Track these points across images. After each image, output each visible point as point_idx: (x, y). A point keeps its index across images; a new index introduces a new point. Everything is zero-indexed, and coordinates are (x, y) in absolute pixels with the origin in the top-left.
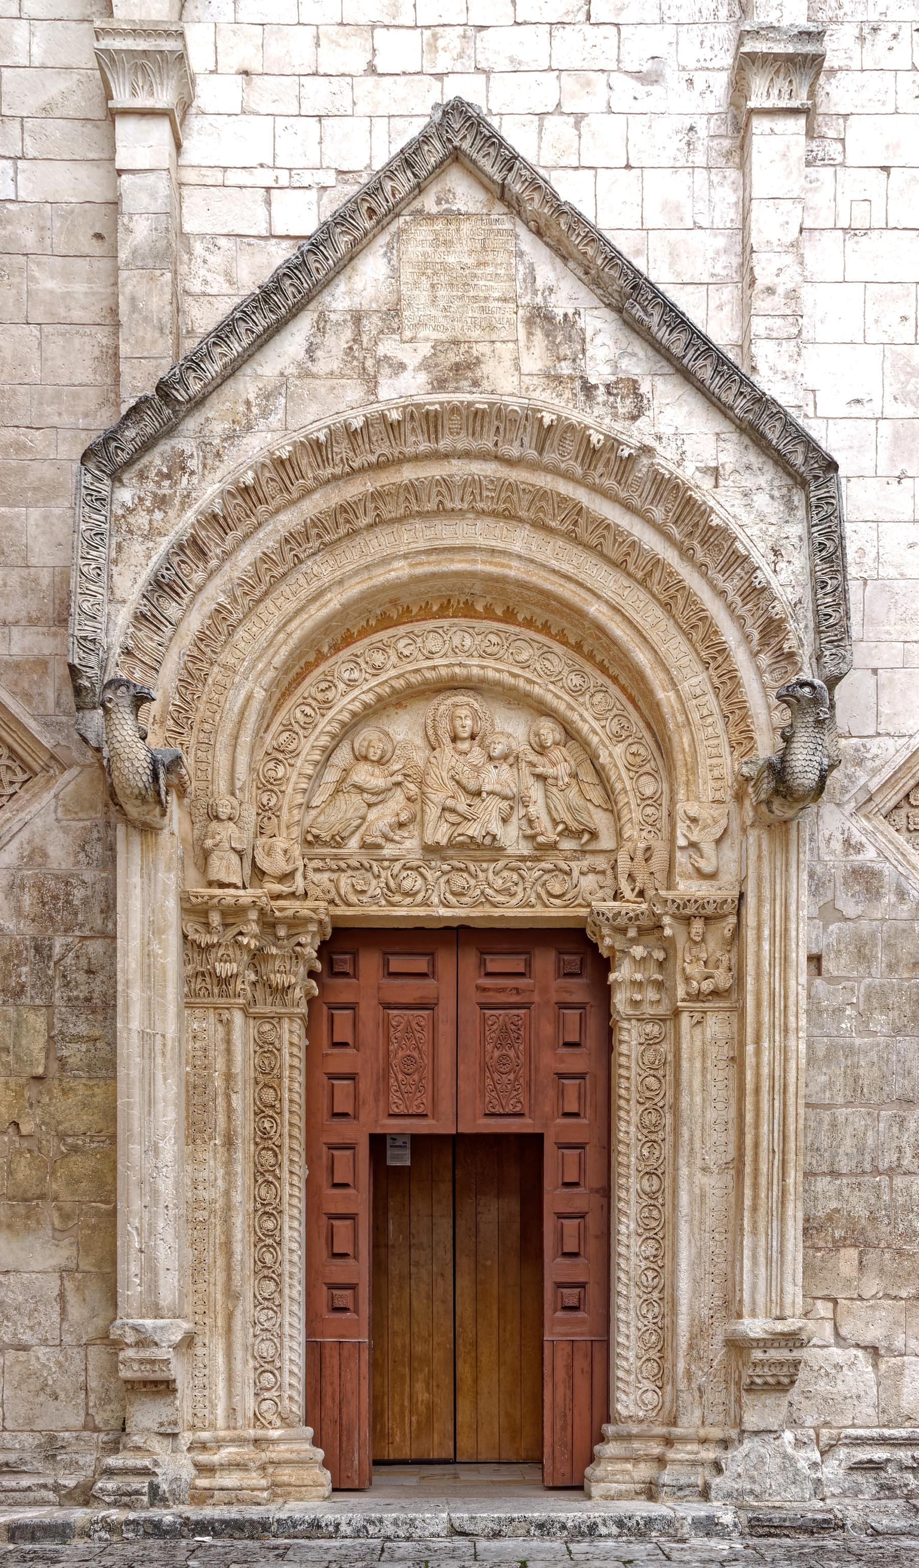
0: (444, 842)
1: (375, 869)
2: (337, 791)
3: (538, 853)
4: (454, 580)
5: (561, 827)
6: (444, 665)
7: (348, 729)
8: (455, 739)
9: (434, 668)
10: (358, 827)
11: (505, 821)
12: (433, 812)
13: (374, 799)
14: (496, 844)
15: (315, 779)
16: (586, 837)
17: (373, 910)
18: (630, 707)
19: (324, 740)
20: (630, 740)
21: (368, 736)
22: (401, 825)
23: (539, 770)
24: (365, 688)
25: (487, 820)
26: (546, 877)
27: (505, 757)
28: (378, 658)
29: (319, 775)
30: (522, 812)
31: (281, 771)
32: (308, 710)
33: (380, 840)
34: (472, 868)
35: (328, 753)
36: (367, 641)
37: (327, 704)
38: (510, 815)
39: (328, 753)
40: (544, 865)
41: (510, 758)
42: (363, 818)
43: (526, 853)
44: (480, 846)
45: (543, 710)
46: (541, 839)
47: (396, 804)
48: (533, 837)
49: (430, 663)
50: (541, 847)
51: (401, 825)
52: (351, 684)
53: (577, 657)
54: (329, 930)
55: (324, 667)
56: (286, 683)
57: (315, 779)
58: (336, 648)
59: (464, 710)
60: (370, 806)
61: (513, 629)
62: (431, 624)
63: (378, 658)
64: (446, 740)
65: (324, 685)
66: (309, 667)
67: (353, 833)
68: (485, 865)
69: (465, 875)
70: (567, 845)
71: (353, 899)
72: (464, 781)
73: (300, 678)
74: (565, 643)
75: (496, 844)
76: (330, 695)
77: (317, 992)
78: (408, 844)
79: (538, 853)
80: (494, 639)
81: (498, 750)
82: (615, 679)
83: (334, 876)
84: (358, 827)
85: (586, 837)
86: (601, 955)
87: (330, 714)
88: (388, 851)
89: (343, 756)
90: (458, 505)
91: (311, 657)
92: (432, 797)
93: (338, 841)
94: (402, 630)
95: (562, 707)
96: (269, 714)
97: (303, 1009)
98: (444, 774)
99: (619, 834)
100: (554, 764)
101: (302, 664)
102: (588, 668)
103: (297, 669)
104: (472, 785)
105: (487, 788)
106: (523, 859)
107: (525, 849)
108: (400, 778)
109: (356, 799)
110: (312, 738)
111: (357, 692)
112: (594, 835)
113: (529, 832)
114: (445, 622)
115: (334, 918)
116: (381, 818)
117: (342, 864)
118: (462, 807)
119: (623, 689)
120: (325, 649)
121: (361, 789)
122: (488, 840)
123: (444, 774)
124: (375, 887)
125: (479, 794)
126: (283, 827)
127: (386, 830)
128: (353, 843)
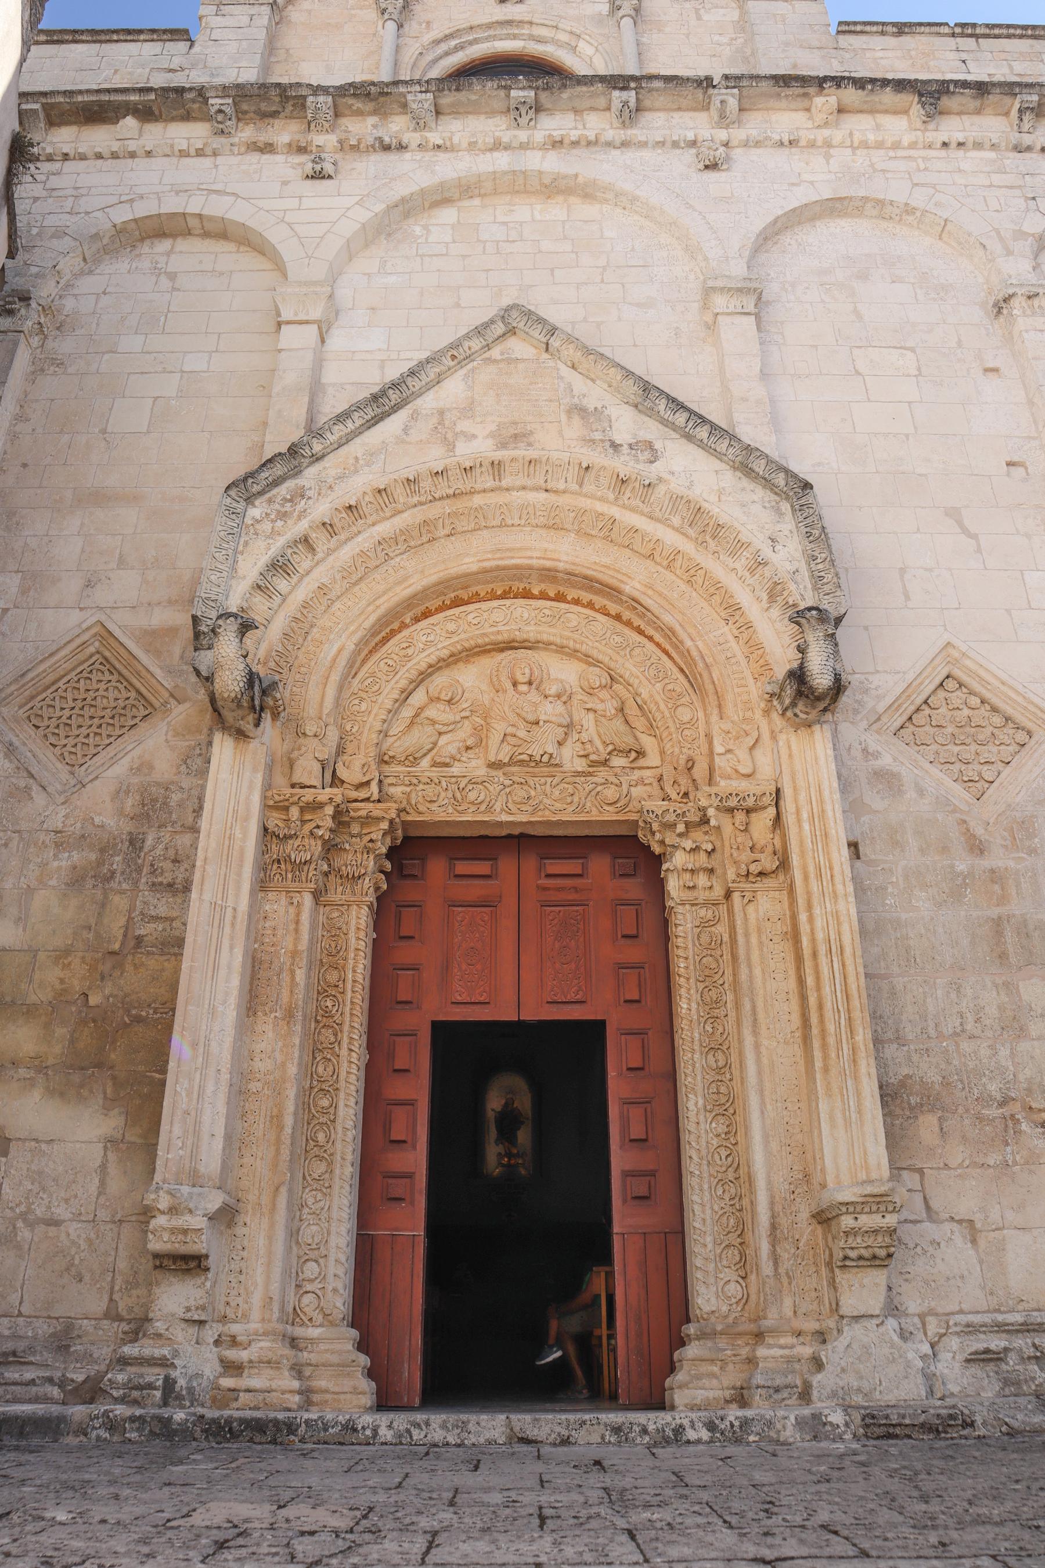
0: (506, 760)
1: (444, 784)
2: (412, 723)
3: (591, 770)
4: (515, 572)
5: (611, 747)
6: (506, 632)
7: (424, 676)
8: (515, 684)
9: (498, 632)
10: (430, 750)
11: (560, 744)
12: (495, 738)
13: (445, 729)
14: (553, 761)
15: (394, 712)
16: (633, 755)
17: (441, 817)
18: (665, 658)
19: (403, 683)
20: (667, 681)
21: (440, 681)
22: (468, 748)
23: (588, 706)
24: (440, 646)
25: (543, 743)
26: (599, 788)
27: (559, 696)
28: (451, 626)
29: (397, 711)
30: (576, 736)
31: (364, 706)
32: (390, 662)
33: (448, 760)
34: (532, 783)
35: (406, 694)
36: (441, 616)
37: (408, 658)
38: (565, 740)
39: (406, 694)
40: (595, 779)
41: (564, 697)
42: (435, 744)
43: (580, 769)
44: (538, 763)
45: (589, 660)
46: (593, 757)
47: (464, 732)
48: (586, 756)
49: (494, 629)
50: (594, 764)
51: (468, 748)
52: (428, 644)
53: (617, 624)
54: (400, 833)
55: (406, 633)
56: (373, 644)
57: (394, 712)
58: (417, 620)
59: (523, 662)
60: (440, 734)
61: (563, 605)
62: (495, 603)
63: (451, 626)
64: (508, 685)
65: (405, 645)
66: (393, 633)
67: (425, 755)
68: (543, 780)
69: (526, 787)
70: (618, 762)
71: (421, 808)
72: (524, 714)
73: (385, 640)
74: (608, 615)
75: (553, 761)
76: (410, 651)
77: (385, 887)
78: (474, 763)
79: (591, 770)
80: (547, 612)
81: (553, 690)
82: (650, 638)
83: (408, 789)
84: (430, 750)
85: (633, 755)
86: (653, 853)
87: (410, 664)
88: (455, 770)
89: (419, 698)
90: (517, 521)
91: (396, 626)
92: (495, 726)
93: (413, 759)
94: (471, 607)
95: (606, 660)
96: (357, 665)
97: (371, 898)
98: (506, 709)
99: (662, 753)
100: (602, 701)
101: (388, 630)
102: (627, 631)
103: (383, 634)
104: (531, 718)
105: (543, 717)
106: (578, 774)
107: (580, 765)
108: (467, 714)
109: (429, 729)
110: (393, 682)
111: (433, 649)
112: (641, 754)
113: (582, 753)
114: (508, 602)
115: (405, 824)
116: (449, 745)
117: (415, 781)
118: (522, 734)
119: (658, 645)
120: (408, 621)
121: (433, 722)
122: (545, 759)
123: (506, 709)
124: (444, 798)
125: (537, 723)
126: (362, 747)
127: (454, 752)
128: (425, 763)
